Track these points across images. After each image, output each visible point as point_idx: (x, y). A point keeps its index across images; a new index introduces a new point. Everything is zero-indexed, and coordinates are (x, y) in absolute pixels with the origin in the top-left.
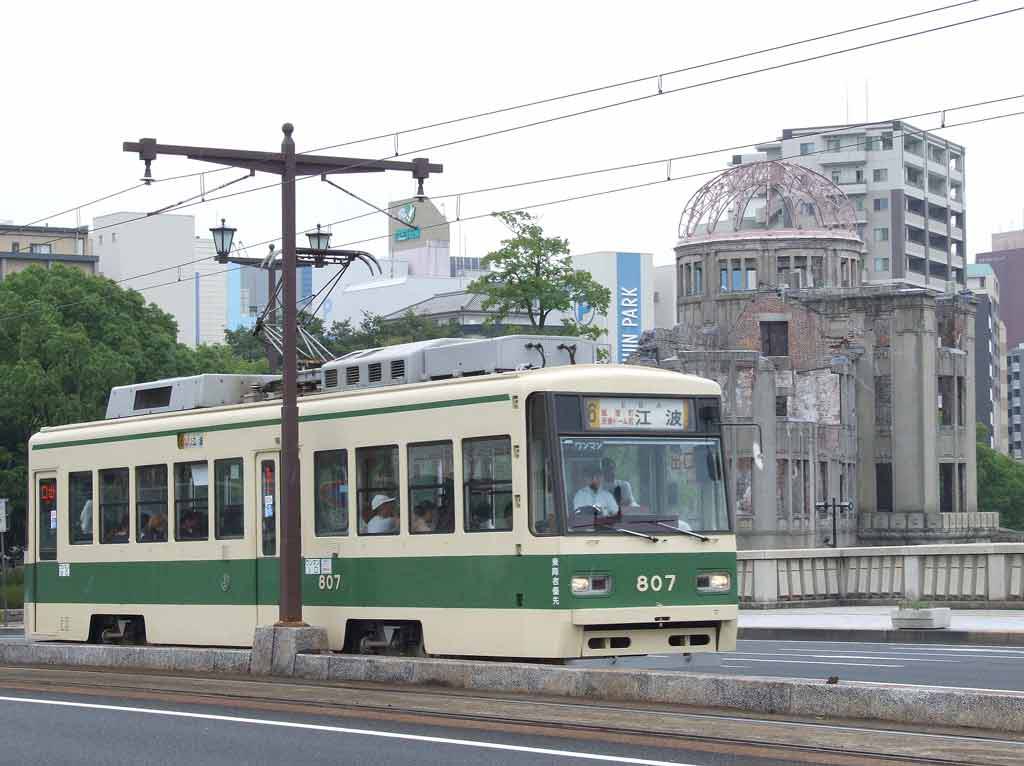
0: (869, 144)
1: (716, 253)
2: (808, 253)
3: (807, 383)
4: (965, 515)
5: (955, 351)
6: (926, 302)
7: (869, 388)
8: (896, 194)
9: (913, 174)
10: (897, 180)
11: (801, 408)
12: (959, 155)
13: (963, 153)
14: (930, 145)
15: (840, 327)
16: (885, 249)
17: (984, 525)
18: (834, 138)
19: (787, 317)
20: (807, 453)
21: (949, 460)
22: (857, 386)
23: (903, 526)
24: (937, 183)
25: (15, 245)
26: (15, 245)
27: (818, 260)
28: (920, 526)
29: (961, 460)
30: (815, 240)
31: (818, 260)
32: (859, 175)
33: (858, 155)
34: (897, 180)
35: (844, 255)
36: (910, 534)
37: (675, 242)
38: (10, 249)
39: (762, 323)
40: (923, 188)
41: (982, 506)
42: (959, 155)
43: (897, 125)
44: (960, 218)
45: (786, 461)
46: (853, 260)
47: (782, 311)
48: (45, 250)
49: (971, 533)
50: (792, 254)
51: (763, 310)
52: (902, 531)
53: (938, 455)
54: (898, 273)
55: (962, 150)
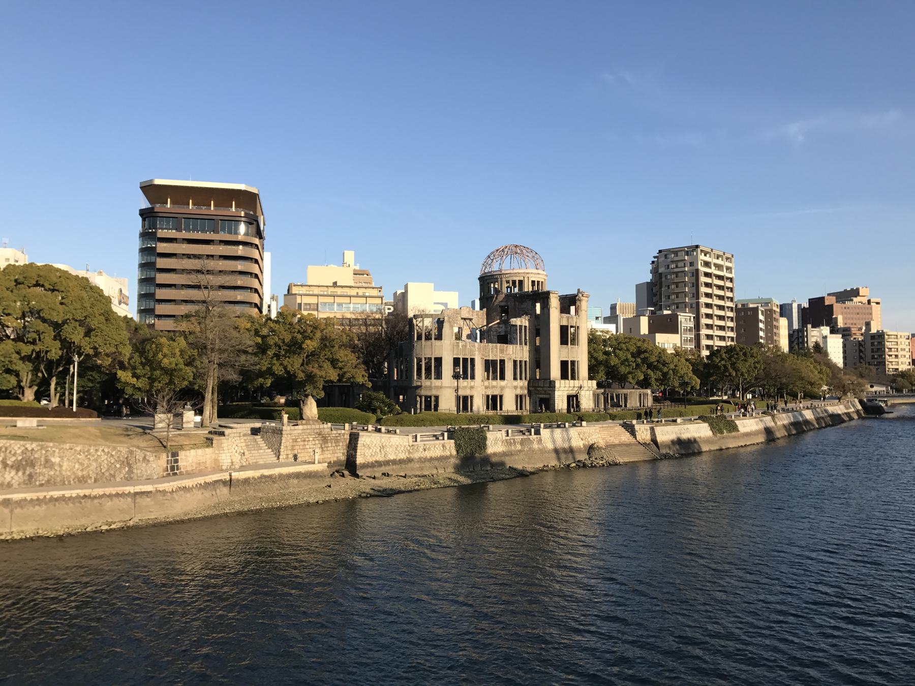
0: (687, 253)
1: (486, 280)
2: (517, 279)
4: (572, 381)
8: (697, 270)
9: (707, 264)
13: (732, 256)
14: (715, 254)
15: (524, 306)
18: (676, 252)
20: (474, 355)
23: (542, 385)
24: (719, 267)
25: (357, 293)
26: (357, 293)
29: (572, 359)
30: (519, 273)
32: (685, 264)
36: (545, 389)
38: (356, 294)
40: (710, 268)
41: (591, 378)
43: (697, 247)
45: (460, 358)
46: (538, 282)
50: (511, 279)
52: (542, 387)
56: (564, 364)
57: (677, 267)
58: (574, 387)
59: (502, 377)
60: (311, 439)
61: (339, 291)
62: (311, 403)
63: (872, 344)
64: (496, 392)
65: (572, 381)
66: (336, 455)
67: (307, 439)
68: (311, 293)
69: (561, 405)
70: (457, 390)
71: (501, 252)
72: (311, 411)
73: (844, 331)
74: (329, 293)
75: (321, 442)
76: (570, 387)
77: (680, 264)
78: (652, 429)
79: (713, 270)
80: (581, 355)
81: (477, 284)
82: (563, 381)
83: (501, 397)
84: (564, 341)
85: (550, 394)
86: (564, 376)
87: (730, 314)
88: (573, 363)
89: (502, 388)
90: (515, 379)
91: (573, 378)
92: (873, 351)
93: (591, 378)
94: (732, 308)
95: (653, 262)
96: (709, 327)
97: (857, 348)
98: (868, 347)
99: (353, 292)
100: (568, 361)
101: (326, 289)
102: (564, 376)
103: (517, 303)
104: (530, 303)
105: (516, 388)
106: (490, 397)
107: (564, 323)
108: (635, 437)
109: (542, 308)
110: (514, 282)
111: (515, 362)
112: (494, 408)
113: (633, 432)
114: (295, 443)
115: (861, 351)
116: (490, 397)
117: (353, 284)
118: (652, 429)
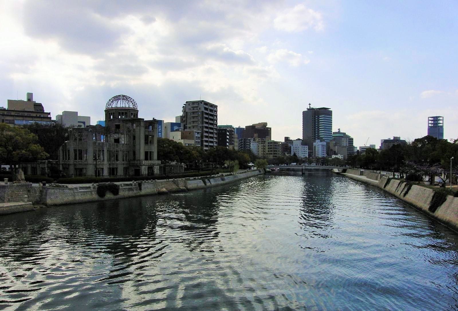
2: (124, 112)
3: (123, 136)
5: (149, 130)
6: (141, 120)
7: (132, 137)
8: (202, 111)
9: (206, 109)
10: (203, 109)
11: (121, 140)
12: (216, 107)
16: (201, 120)
17: (156, 163)
18: (193, 103)
19: (120, 124)
20: (104, 148)
21: (147, 151)
22: (130, 136)
24: (211, 111)
25: (36, 115)
27: (126, 113)
28: (139, 163)
29: (150, 151)
31: (126, 113)
33: (197, 106)
34: (203, 109)
35: (132, 112)
37: (105, 109)
38: (35, 116)
39: (116, 125)
40: (208, 111)
41: (158, 159)
42: (216, 107)
43: (203, 101)
44: (217, 116)
47: (119, 122)
48: (42, 116)
49: (152, 165)
50: (121, 112)
51: (116, 122)
53: (144, 150)
54: (202, 124)
55: (217, 106)
56: (146, 153)
57: (194, 110)
58: (151, 164)
59: (117, 160)
60: (21, 191)
61: (26, 114)
62: (21, 173)
63: (268, 146)
64: (115, 167)
65: (150, 161)
66: (36, 198)
67: (19, 191)
68: (10, 114)
69: (145, 172)
70: (96, 166)
71: (117, 98)
72: (21, 177)
73: (258, 140)
74: (20, 115)
75: (27, 192)
76: (149, 164)
77: (196, 109)
78: (185, 183)
79: (208, 112)
80: (154, 149)
81: (104, 114)
82: (146, 161)
83: (117, 168)
84: (146, 142)
85: (140, 167)
86: (146, 159)
87: (215, 132)
88: (151, 152)
89: (117, 164)
90: (123, 160)
91: (151, 160)
92: (268, 148)
93: (158, 159)
94: (216, 129)
95: (183, 107)
96: (206, 137)
97: (263, 147)
98: (267, 147)
99: (34, 115)
100: (148, 152)
101: (18, 113)
102: (146, 159)
103: (124, 123)
104: (131, 123)
105: (124, 164)
106: (111, 169)
107: (147, 134)
108: (178, 186)
109: (137, 126)
110: (123, 113)
111: (123, 152)
112: (113, 174)
113: (178, 185)
114: (13, 193)
115: (264, 149)
116: (111, 169)
117: (33, 110)
118: (185, 183)
